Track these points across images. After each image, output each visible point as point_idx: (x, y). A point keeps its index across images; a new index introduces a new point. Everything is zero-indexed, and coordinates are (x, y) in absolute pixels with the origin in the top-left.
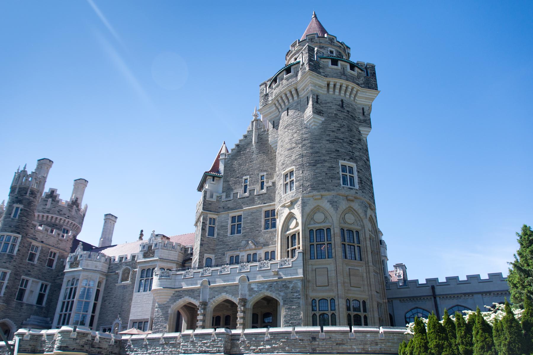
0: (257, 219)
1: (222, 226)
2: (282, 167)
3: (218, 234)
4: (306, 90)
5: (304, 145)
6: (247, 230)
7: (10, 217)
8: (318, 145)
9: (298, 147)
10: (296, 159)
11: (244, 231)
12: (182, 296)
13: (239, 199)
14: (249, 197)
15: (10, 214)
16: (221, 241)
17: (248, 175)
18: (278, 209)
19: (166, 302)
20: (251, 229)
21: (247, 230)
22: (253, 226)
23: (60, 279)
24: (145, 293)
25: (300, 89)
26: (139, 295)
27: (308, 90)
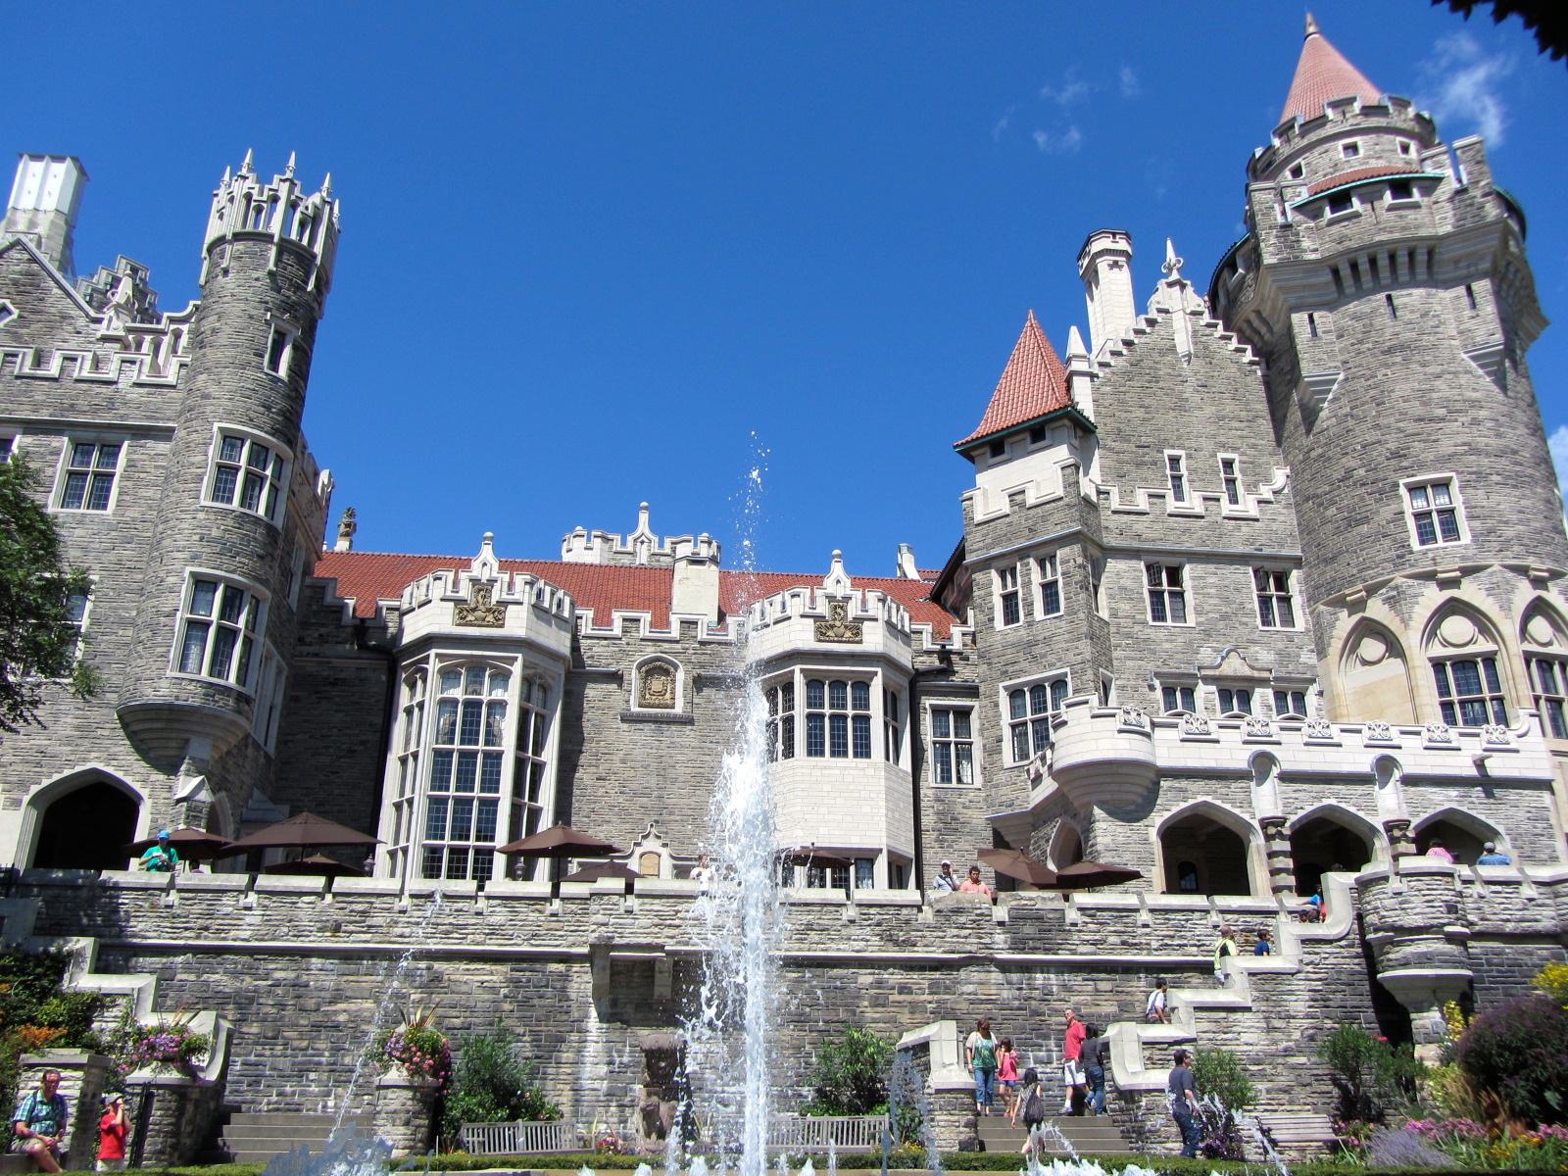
0: (1236, 589)
1: (1123, 589)
2: (1393, 462)
3: (1114, 614)
4: (1468, 266)
5: (1475, 422)
6: (1211, 615)
7: (261, 369)
8: (1510, 433)
9: (1456, 421)
10: (1455, 454)
11: (1202, 619)
12: (1189, 794)
13: (1170, 515)
14: (1202, 517)
15: (262, 356)
16: (1128, 636)
17: (1184, 448)
18: (1392, 580)
19: (1132, 807)
20: (1224, 617)
21: (1211, 615)
22: (1228, 610)
23: (316, 655)
24: (840, 761)
25: (1446, 256)
26: (825, 768)
27: (1472, 269)
